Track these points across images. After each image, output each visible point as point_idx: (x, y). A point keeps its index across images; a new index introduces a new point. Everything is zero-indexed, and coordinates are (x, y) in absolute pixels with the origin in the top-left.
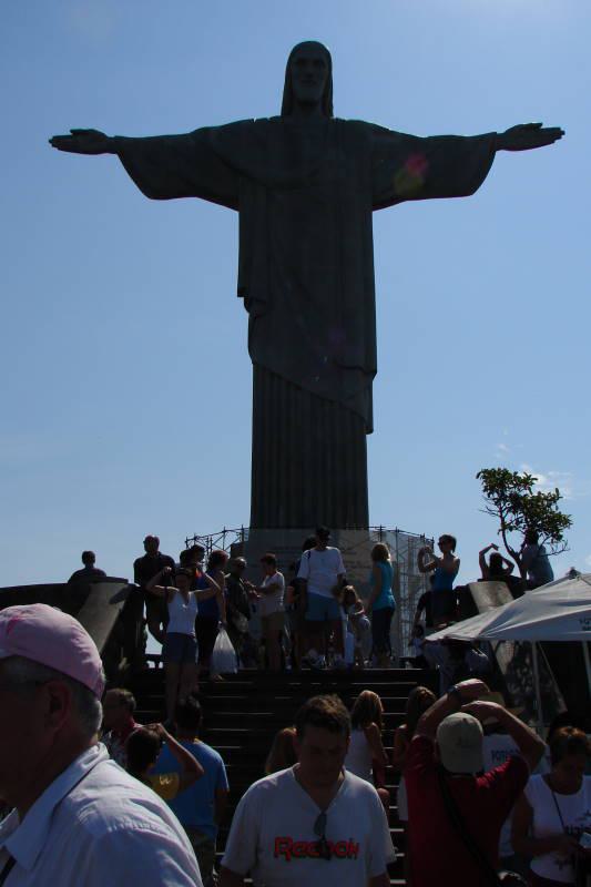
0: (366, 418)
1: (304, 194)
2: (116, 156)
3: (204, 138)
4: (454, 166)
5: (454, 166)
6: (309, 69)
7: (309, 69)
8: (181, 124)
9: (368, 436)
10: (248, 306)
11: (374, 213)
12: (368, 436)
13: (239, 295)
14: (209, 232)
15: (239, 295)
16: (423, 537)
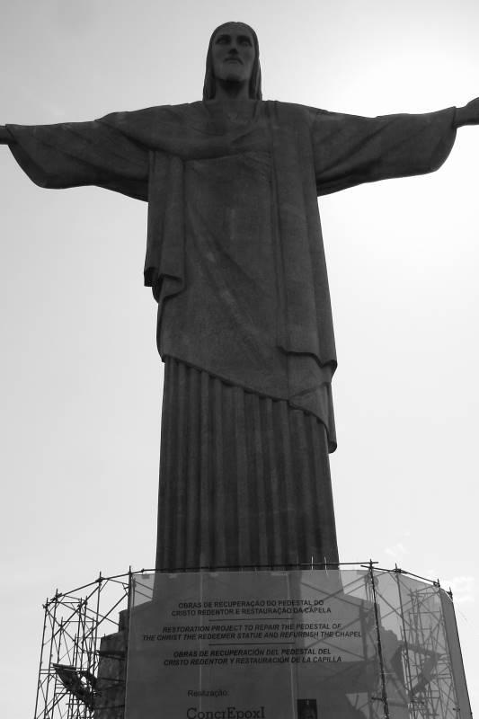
0: (327, 423)
1: (230, 189)
2: (6, 146)
3: (113, 124)
4: (408, 146)
5: (408, 146)
6: (233, 50)
7: (233, 50)
8: (87, 111)
9: (330, 455)
10: (157, 296)
11: (318, 198)
12: (330, 455)
13: (147, 284)
14: (115, 225)
15: (147, 284)
16: (437, 584)
